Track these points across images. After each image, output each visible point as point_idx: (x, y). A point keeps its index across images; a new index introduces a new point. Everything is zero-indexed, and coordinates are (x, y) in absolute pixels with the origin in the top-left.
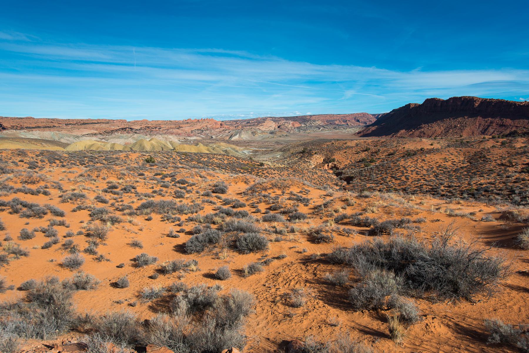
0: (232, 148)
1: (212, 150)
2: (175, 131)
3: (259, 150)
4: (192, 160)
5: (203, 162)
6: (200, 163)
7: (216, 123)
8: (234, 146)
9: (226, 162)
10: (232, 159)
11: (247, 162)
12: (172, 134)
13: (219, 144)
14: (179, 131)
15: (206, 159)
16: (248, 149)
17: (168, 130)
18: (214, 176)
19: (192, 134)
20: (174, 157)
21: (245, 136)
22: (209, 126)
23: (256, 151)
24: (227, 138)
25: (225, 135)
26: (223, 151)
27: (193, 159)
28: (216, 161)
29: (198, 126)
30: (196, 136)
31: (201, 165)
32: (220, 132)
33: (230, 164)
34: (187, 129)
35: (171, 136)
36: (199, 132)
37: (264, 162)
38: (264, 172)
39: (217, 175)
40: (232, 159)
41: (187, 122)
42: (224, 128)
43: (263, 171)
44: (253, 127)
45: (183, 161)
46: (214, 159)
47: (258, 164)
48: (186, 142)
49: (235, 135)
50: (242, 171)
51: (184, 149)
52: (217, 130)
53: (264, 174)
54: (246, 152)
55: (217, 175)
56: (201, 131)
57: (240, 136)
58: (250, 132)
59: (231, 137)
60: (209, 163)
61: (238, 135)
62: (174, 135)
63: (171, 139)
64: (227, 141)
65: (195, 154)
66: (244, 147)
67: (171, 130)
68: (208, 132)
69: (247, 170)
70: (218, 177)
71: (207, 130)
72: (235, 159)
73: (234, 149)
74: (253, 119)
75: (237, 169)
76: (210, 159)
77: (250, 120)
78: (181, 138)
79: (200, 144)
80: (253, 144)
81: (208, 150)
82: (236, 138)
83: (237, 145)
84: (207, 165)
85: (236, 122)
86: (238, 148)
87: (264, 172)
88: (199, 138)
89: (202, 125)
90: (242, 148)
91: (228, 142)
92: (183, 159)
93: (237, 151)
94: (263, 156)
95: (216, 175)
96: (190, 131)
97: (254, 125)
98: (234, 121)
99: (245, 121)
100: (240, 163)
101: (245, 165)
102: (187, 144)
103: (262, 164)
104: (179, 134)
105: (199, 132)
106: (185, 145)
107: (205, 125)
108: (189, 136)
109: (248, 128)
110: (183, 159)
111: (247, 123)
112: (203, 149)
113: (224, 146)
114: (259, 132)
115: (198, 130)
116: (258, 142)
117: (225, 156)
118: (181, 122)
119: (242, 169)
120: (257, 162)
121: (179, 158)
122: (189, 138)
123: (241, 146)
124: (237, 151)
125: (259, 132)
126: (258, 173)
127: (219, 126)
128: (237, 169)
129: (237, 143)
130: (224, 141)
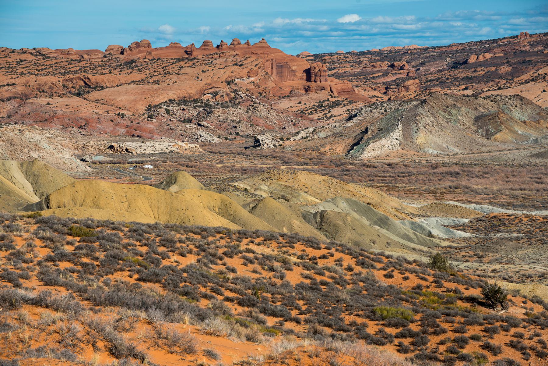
0: (354, 204)
1: (244, 213)
2: (64, 104)
3: (512, 219)
4: (114, 261)
5: (173, 280)
6: (154, 278)
7: (282, 66)
8: (370, 194)
9: (294, 277)
10: (330, 263)
11: (414, 281)
12: (44, 120)
13: (286, 180)
14: (86, 108)
15: (191, 260)
16: (448, 211)
17: (24, 98)
18: (190, 351)
19: (151, 126)
20: (20, 245)
21: (435, 140)
22: (244, 83)
23: (495, 224)
24: (339, 149)
25: (328, 134)
26: (305, 217)
27: (116, 258)
28: (243, 271)
29: (186, 84)
30: (171, 132)
31: (154, 290)
32: (301, 114)
33: (314, 287)
34: (126, 94)
35: (35, 135)
36: (191, 112)
37: (504, 285)
38: (499, 340)
39: (213, 344)
40: (330, 263)
41: (130, 60)
42: (323, 96)
43: (491, 332)
44: (488, 89)
45: (64, 265)
46: (235, 262)
47: (476, 292)
48: (118, 165)
49: (384, 131)
50: (372, 328)
51: (96, 205)
52: (285, 104)
53: (495, 350)
54: (434, 225)
55: (213, 344)
56: (200, 108)
57: (407, 135)
58: (465, 117)
59: (358, 143)
60: (205, 278)
61: (397, 133)
62: (56, 129)
63: (36, 147)
64: (338, 163)
65: (137, 231)
66: (430, 201)
67: (43, 100)
68: (235, 113)
69: (401, 322)
70: (210, 354)
71: (234, 102)
72: (348, 261)
73: (367, 209)
74: (487, 46)
75: (348, 319)
76: (214, 257)
77: (470, 48)
78: (92, 143)
79: (188, 181)
80: (477, 184)
81: (225, 211)
82: (383, 148)
83: (390, 189)
84: (184, 289)
85: (392, 58)
86: (390, 203)
87: (499, 340)
88: (185, 147)
89: (206, 79)
90: (413, 206)
91: (342, 170)
92: (63, 257)
93: (383, 222)
94: (531, 251)
95: (202, 343)
96: (142, 108)
97: (489, 78)
98: (381, 55)
99: (440, 53)
100: (370, 282)
101: (396, 295)
102: (120, 176)
103: (493, 298)
104: (84, 125)
105: (191, 112)
106: (104, 185)
107: (225, 74)
108: (135, 133)
109: (458, 91)
110: (63, 257)
111: (455, 66)
112: (198, 205)
113: (313, 190)
114: (517, 114)
115: (183, 102)
116: (511, 170)
117: (298, 248)
118: (97, 59)
119: (372, 315)
120: (469, 284)
121: (42, 253)
122: (135, 146)
123: (411, 193)
124: (383, 222)
125: (517, 114)
126: (462, 342)
127: (297, 82)
128: (348, 319)
129: (390, 177)
130: (317, 161)
